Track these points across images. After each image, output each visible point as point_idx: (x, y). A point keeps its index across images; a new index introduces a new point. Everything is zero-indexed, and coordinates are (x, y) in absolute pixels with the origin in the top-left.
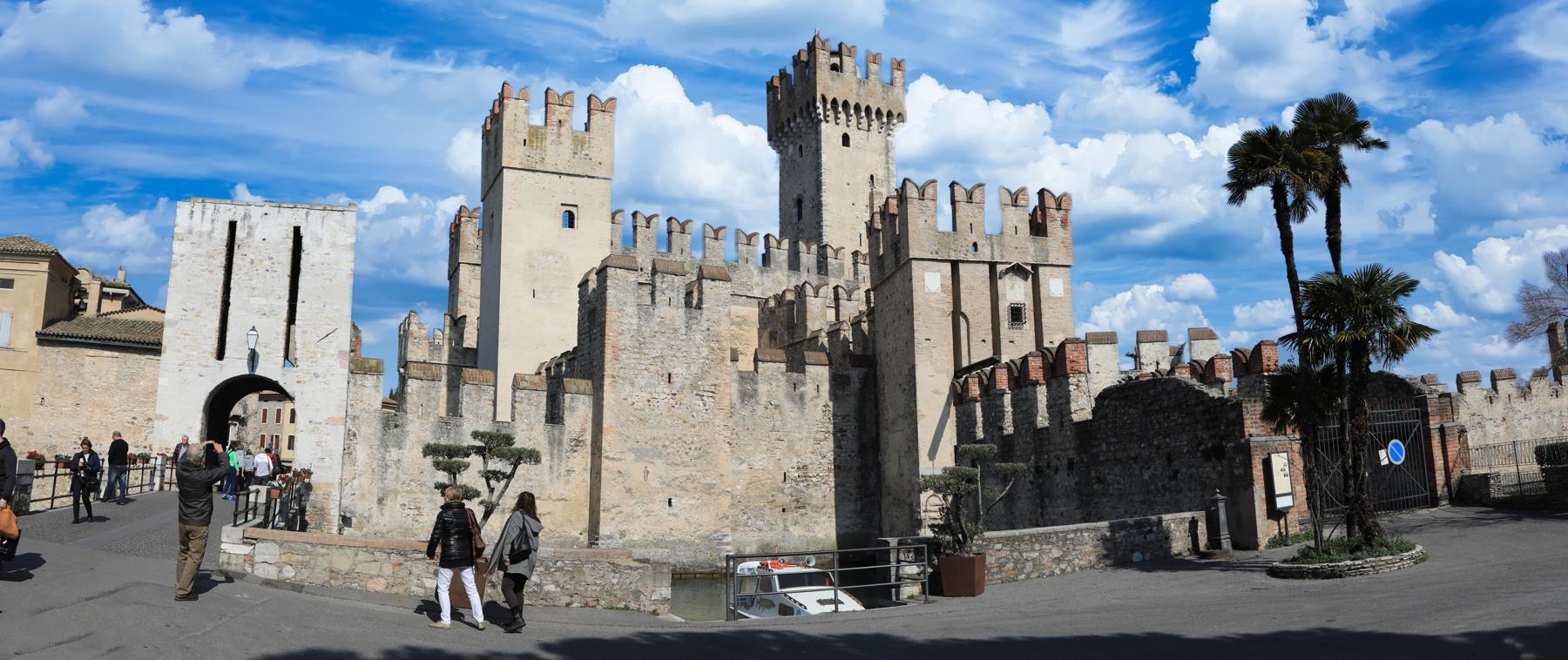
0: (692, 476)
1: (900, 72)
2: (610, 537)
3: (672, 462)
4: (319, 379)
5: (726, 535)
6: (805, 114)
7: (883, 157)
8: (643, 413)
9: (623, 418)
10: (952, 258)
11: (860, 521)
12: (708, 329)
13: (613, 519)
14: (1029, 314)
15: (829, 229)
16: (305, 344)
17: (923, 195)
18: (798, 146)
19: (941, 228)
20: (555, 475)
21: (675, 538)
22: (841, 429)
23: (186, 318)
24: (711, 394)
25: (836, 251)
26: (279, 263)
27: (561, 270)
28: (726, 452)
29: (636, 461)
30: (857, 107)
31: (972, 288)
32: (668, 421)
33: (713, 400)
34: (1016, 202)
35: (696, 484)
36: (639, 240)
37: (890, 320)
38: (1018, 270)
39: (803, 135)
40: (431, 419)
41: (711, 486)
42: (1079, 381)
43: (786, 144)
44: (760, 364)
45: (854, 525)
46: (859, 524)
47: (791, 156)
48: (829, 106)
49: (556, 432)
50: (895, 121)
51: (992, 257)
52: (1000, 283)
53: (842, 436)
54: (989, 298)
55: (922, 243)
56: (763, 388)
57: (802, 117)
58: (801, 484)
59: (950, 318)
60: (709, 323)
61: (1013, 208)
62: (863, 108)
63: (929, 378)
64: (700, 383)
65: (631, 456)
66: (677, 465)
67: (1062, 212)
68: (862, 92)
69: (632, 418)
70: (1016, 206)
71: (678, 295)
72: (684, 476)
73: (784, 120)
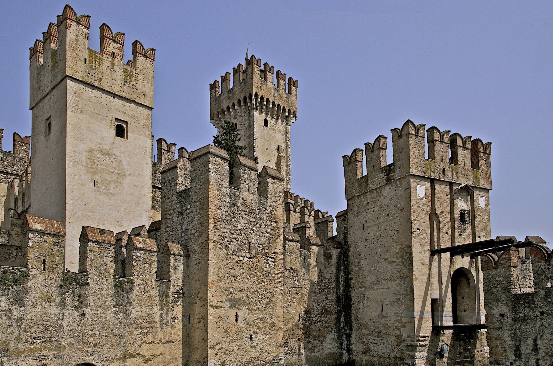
1: (295, 88)
8: (234, 271)
9: (222, 275)
12: (271, 213)
17: (418, 133)
20: (165, 321)
24: (273, 260)
29: (230, 308)
30: (274, 104)
33: (274, 264)
39: (238, 117)
44: (287, 242)
48: (259, 100)
57: (240, 105)
62: (276, 105)
64: (267, 251)
65: (228, 304)
68: (276, 95)
69: (227, 275)
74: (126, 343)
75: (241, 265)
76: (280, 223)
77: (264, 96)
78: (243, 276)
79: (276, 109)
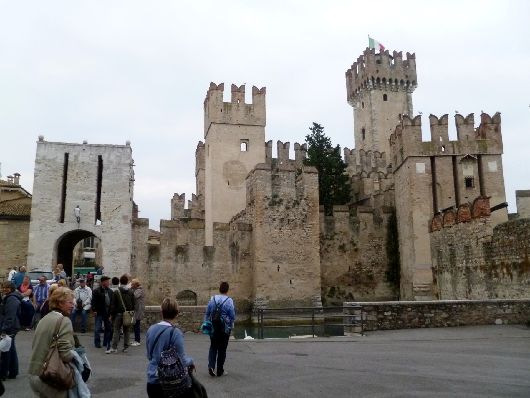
0: (301, 269)
2: (262, 299)
3: (291, 263)
4: (114, 230)
5: (319, 297)
6: (364, 87)
7: (406, 104)
9: (266, 242)
10: (431, 155)
11: (389, 291)
13: (263, 290)
14: (476, 182)
15: (378, 143)
16: (105, 213)
18: (362, 103)
19: (424, 140)
20: (235, 270)
21: (294, 299)
22: (378, 244)
23: (43, 202)
24: (310, 229)
25: (382, 155)
26: (91, 174)
27: (241, 171)
28: (318, 257)
29: (273, 262)
31: (442, 170)
32: (289, 242)
34: (466, 122)
35: (304, 273)
36: (280, 155)
37: (401, 189)
38: (468, 158)
39: (364, 97)
40: (173, 246)
41: (311, 274)
42: (486, 220)
43: (356, 102)
45: (386, 293)
46: (388, 292)
47: (359, 108)
48: (375, 81)
49: (235, 250)
50: (411, 85)
51: (454, 152)
52: (459, 166)
53: (379, 248)
54: (453, 175)
55: (414, 148)
56: (337, 225)
57: (362, 88)
58: (358, 272)
59: (431, 187)
60: (308, 194)
61: (465, 125)
62: (394, 80)
63: (420, 218)
65: (271, 260)
66: (294, 263)
67: (495, 125)
68: (392, 72)
70: (467, 124)
71: (292, 181)
72: (297, 269)
73: (354, 90)
74: (210, 281)
75: (282, 235)
76: (316, 203)
77: (380, 77)
78: (284, 241)
79: (394, 83)
